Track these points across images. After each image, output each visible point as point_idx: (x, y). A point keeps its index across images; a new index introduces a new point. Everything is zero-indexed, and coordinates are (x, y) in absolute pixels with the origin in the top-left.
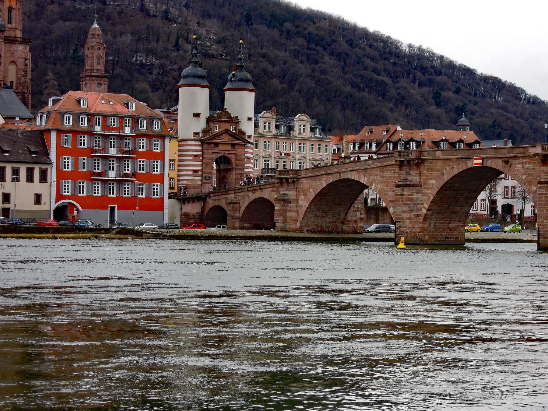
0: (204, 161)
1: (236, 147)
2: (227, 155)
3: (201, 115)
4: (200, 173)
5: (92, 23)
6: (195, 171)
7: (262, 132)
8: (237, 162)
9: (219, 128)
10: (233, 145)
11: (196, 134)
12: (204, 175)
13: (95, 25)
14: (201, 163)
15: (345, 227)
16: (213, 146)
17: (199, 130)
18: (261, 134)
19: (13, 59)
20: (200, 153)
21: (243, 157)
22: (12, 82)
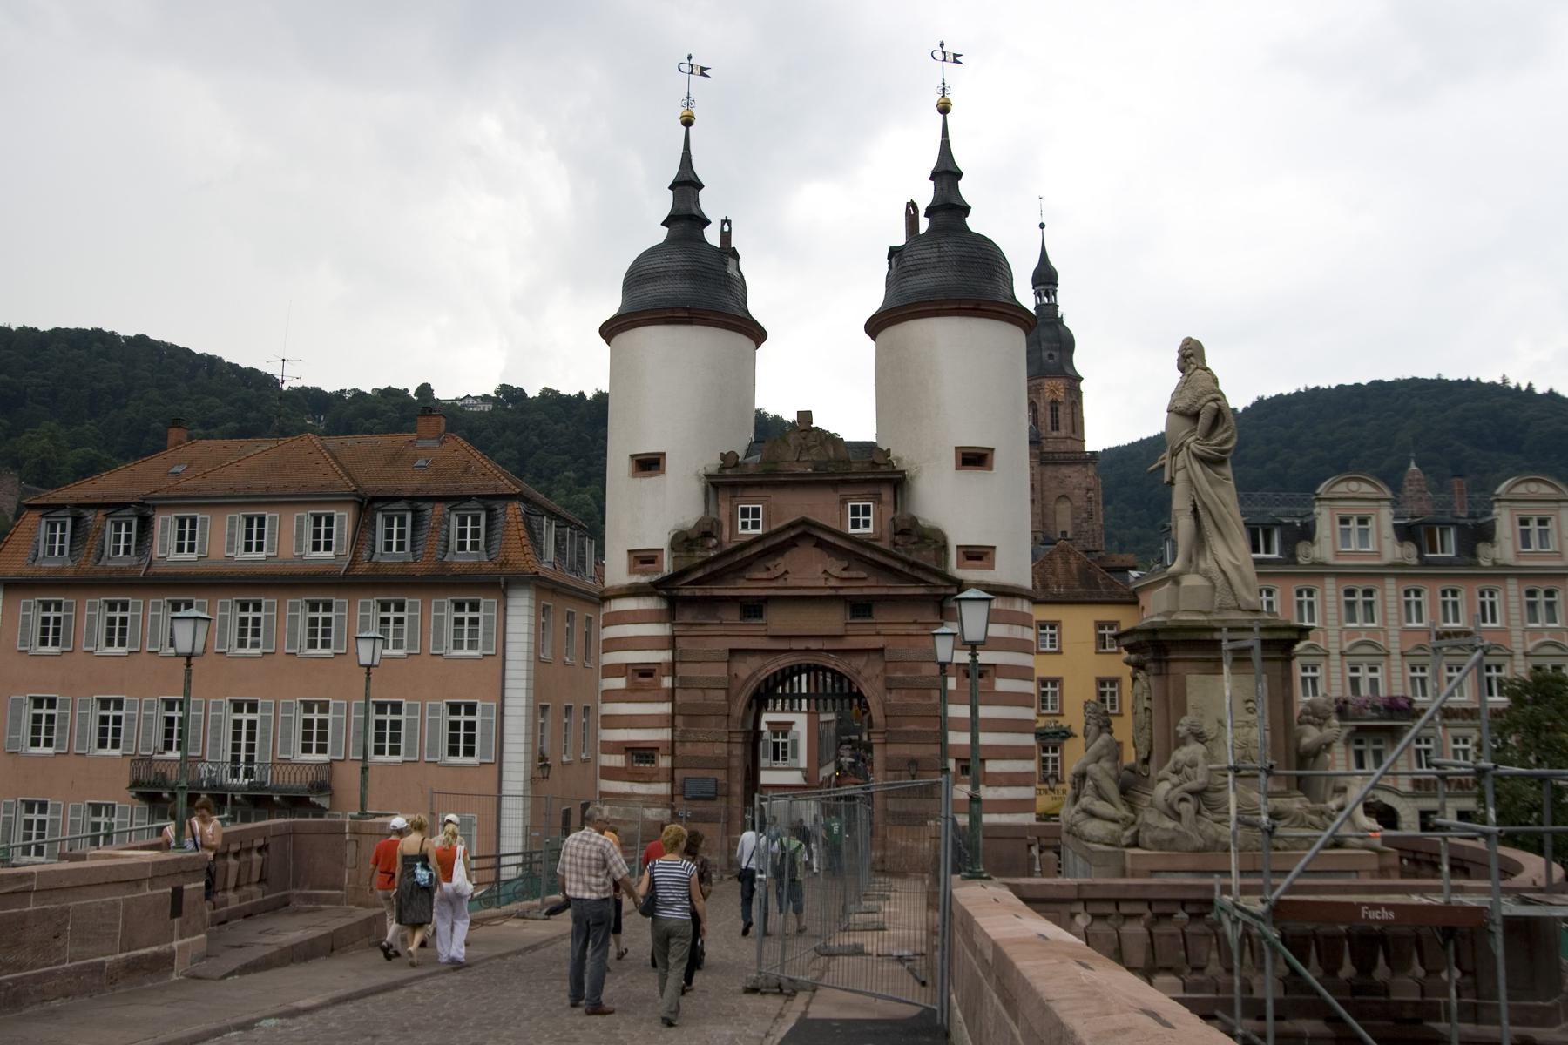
0: (680, 696)
1: (880, 615)
2: (832, 662)
3: (669, 463)
4: (664, 762)
5: (1408, 465)
6: (641, 754)
7: (1329, 558)
8: (893, 698)
9: (768, 521)
10: (861, 607)
12: (678, 774)
13: (1413, 467)
14: (665, 708)
16: (733, 615)
17: (657, 539)
18: (1323, 564)
19: (1062, 492)
20: (664, 656)
21: (931, 670)
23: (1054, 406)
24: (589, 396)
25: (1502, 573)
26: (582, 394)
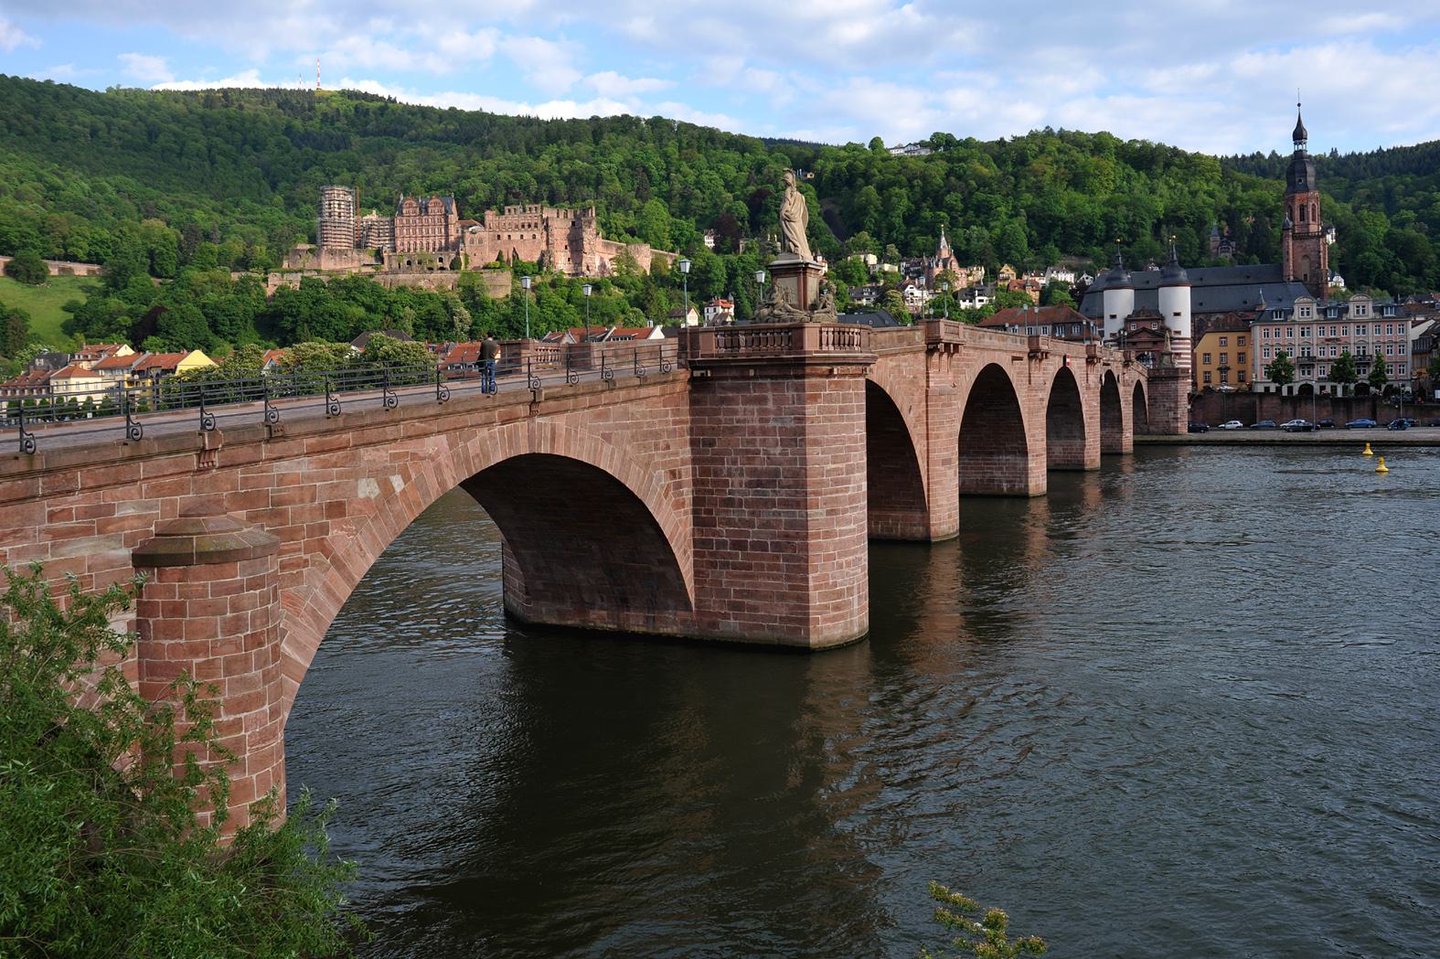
7: (1297, 319)
11: (1112, 335)
15: (1152, 428)
22: (1305, 275)
23: (1302, 208)
24: (1008, 139)
25: (1349, 321)
26: (1002, 139)
